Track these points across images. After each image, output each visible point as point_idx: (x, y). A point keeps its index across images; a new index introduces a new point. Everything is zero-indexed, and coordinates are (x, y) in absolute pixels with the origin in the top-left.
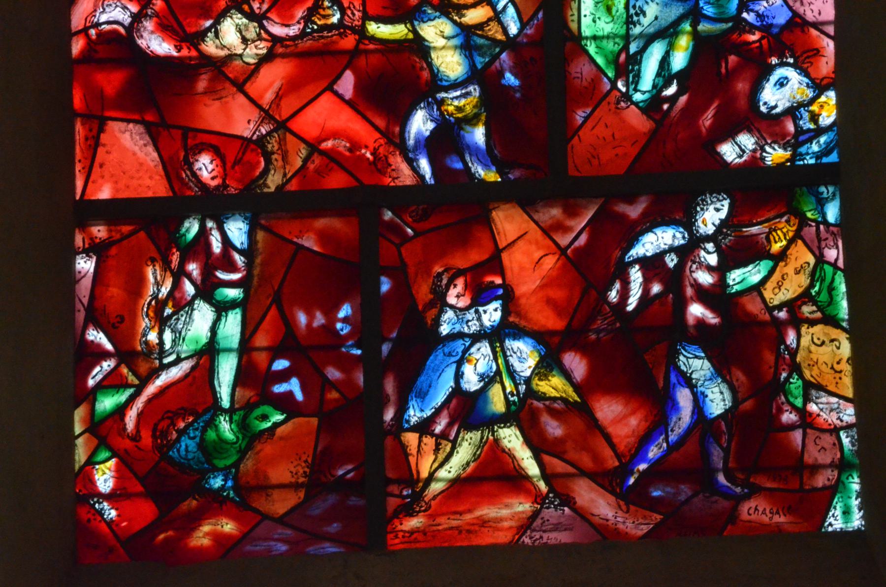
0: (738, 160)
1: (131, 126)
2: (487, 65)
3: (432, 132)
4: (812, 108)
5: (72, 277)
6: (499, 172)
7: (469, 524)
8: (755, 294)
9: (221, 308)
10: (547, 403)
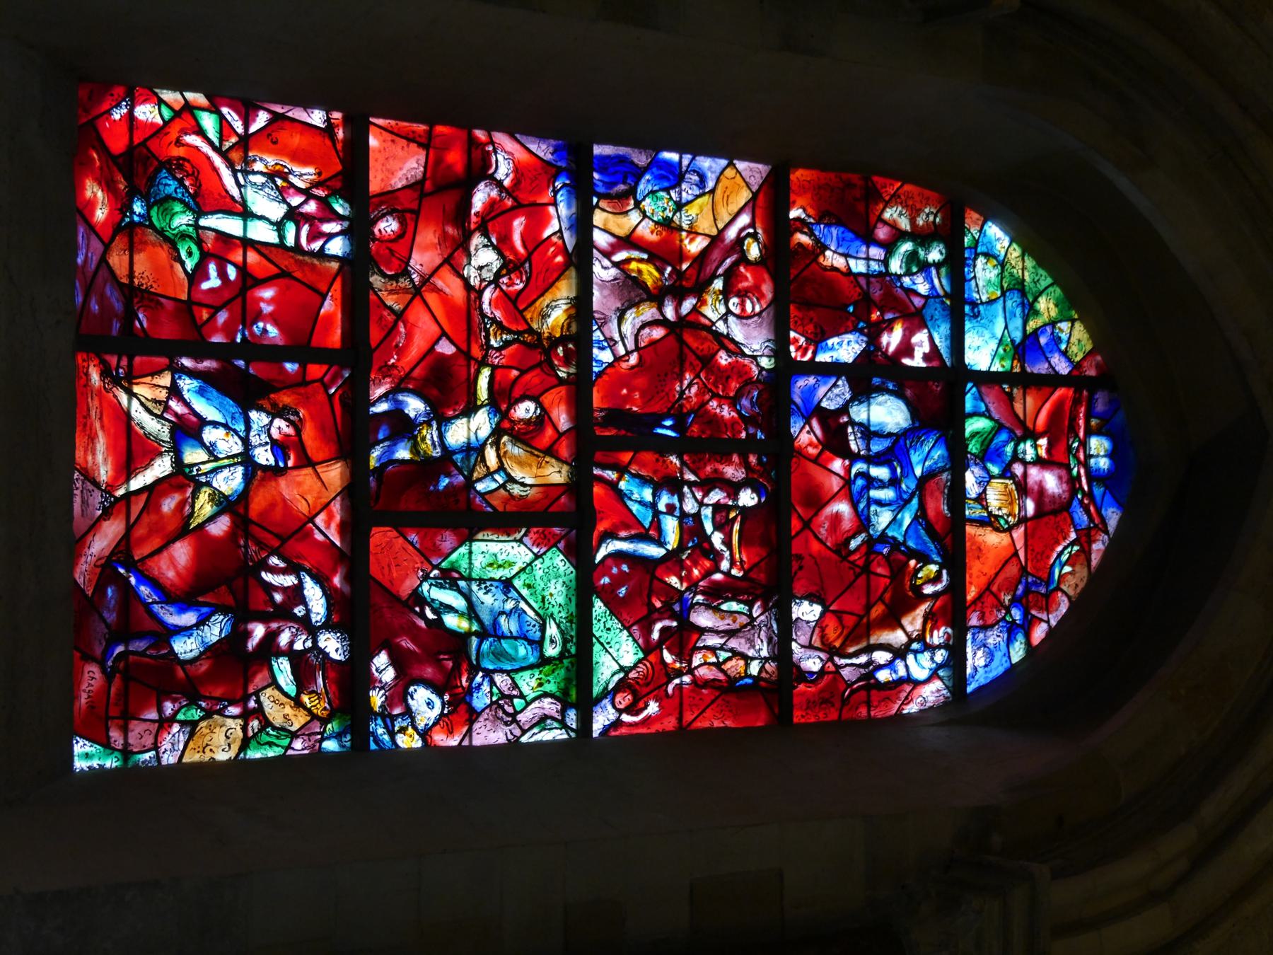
0: (374, 669)
1: (422, 169)
2: (455, 464)
3: (408, 415)
4: (410, 728)
5: (308, 105)
7: (92, 425)
8: (270, 681)
9: (279, 226)
10: (190, 500)
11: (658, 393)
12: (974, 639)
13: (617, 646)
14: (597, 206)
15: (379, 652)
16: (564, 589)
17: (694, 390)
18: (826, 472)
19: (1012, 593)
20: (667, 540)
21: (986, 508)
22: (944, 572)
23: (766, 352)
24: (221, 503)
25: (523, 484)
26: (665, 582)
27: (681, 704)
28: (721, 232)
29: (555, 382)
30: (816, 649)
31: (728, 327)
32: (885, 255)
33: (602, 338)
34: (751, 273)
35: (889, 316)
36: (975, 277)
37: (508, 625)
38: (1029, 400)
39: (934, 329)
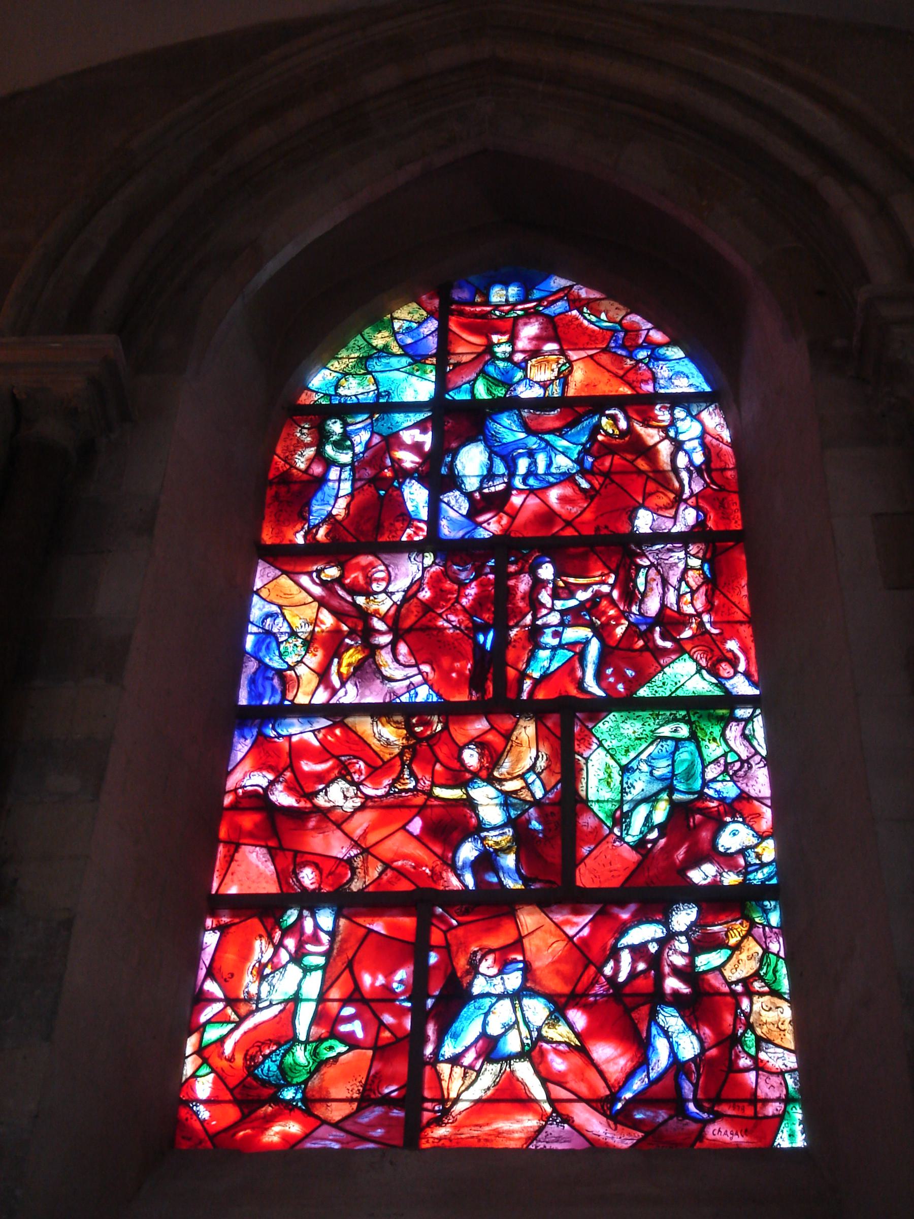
1: (258, 849)
2: (519, 816)
3: (476, 857)
4: (756, 850)
5: (199, 947)
7: (486, 1134)
9: (307, 970)
10: (554, 1045)
11: (455, 648)
13: (679, 676)
14: (292, 701)
15: (689, 877)
16: (629, 722)
17: (452, 618)
19: (624, 359)
20: (584, 637)
21: (552, 381)
22: (607, 412)
23: (419, 559)
24: (556, 1018)
26: (621, 638)
28: (315, 599)
29: (446, 732)
30: (676, 513)
31: (398, 591)
32: (336, 466)
33: (407, 695)
35: (388, 462)
36: (355, 396)
37: (662, 768)
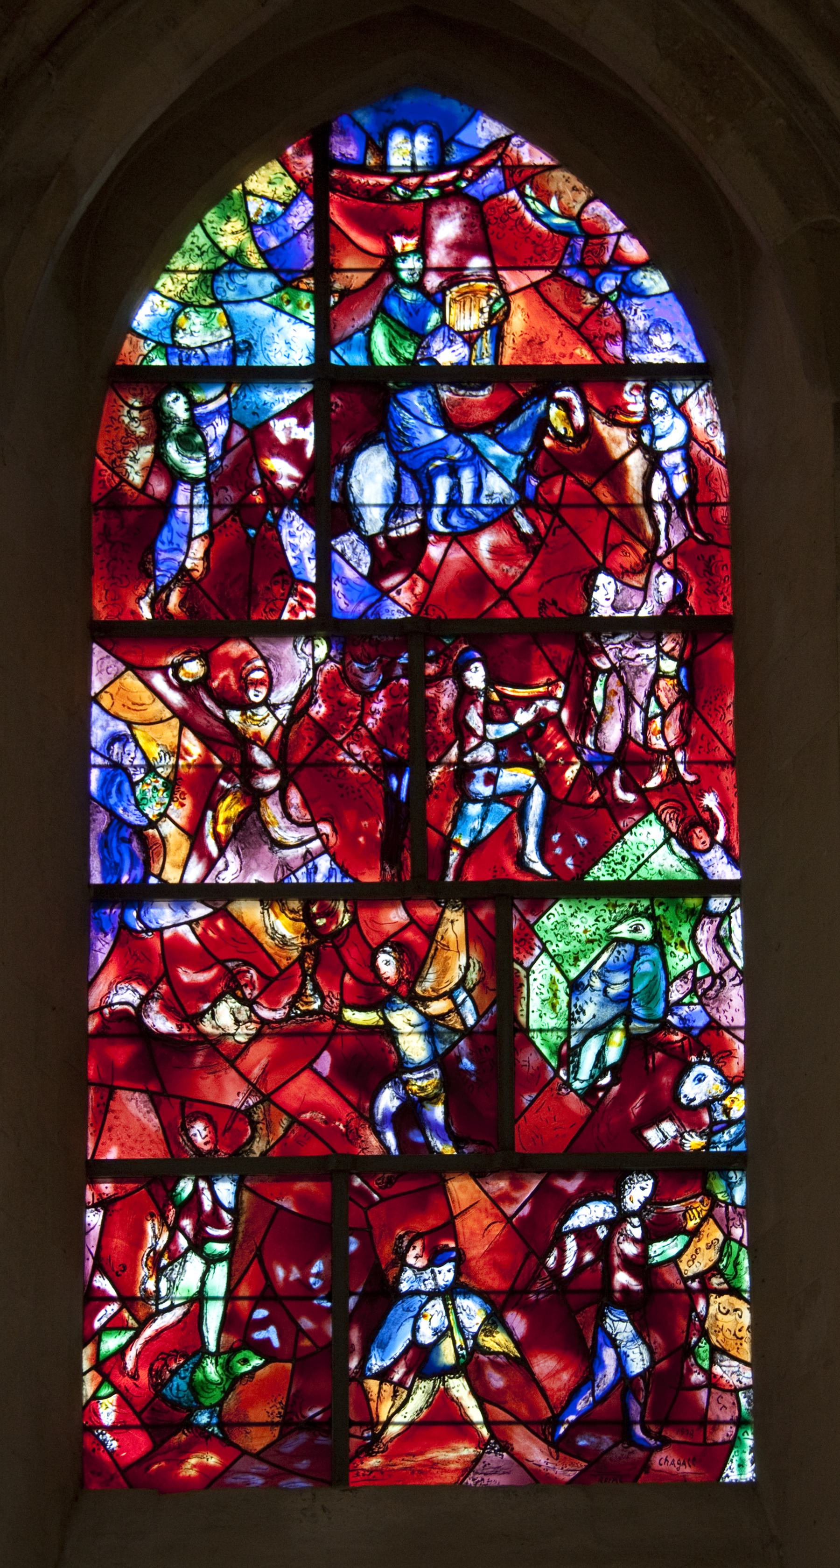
0: (661, 1145)
2: (448, 1051)
6: (457, 1147)
7: (420, 1465)
10: (491, 1357)
12: (640, 350)
13: (642, 847)
15: (645, 1139)
16: (580, 915)
17: (356, 749)
18: (444, 568)
19: (583, 291)
21: (481, 331)
22: (558, 395)
23: (308, 649)
24: (494, 1323)
25: (467, 967)
26: (572, 785)
27: (707, 763)
28: (176, 713)
29: (355, 926)
31: (283, 704)
32: (185, 482)
33: (304, 869)
34: (220, 672)
35: (257, 478)
36: (201, 348)
37: (618, 983)
38: (348, 263)
39: (269, 411)
